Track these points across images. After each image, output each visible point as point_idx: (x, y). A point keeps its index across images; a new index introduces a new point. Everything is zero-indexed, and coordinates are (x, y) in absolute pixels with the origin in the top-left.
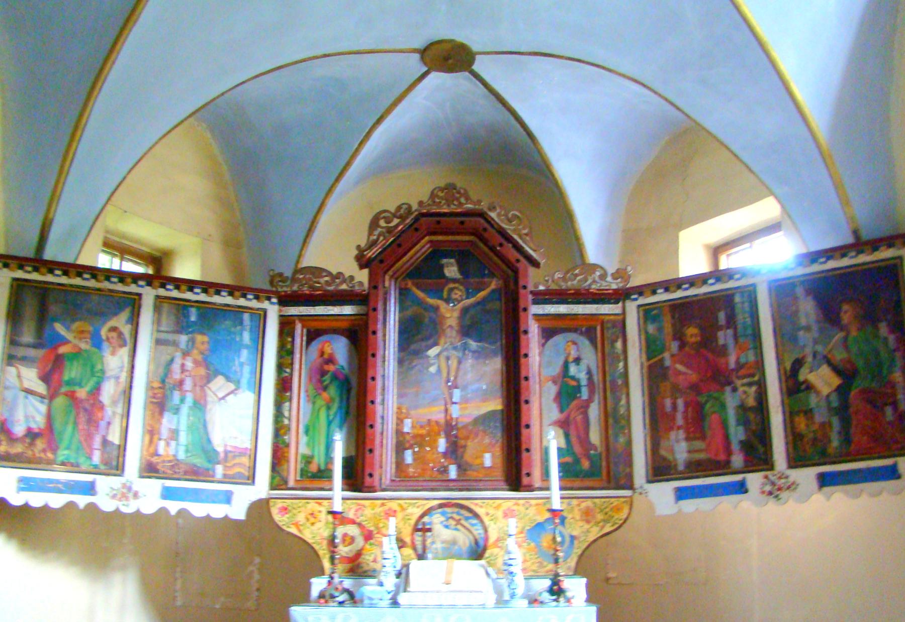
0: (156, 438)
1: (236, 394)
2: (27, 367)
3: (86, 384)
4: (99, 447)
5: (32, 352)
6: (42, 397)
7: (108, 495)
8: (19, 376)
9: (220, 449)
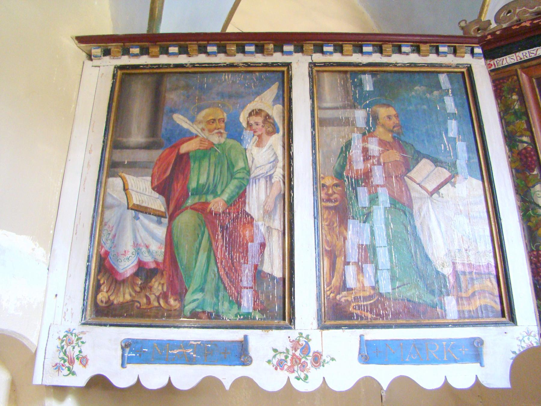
0: (340, 261)
1: (453, 185)
2: (136, 175)
3: (223, 191)
4: (251, 284)
5: (143, 156)
6: (159, 215)
7: (269, 362)
8: (125, 189)
9: (447, 271)
